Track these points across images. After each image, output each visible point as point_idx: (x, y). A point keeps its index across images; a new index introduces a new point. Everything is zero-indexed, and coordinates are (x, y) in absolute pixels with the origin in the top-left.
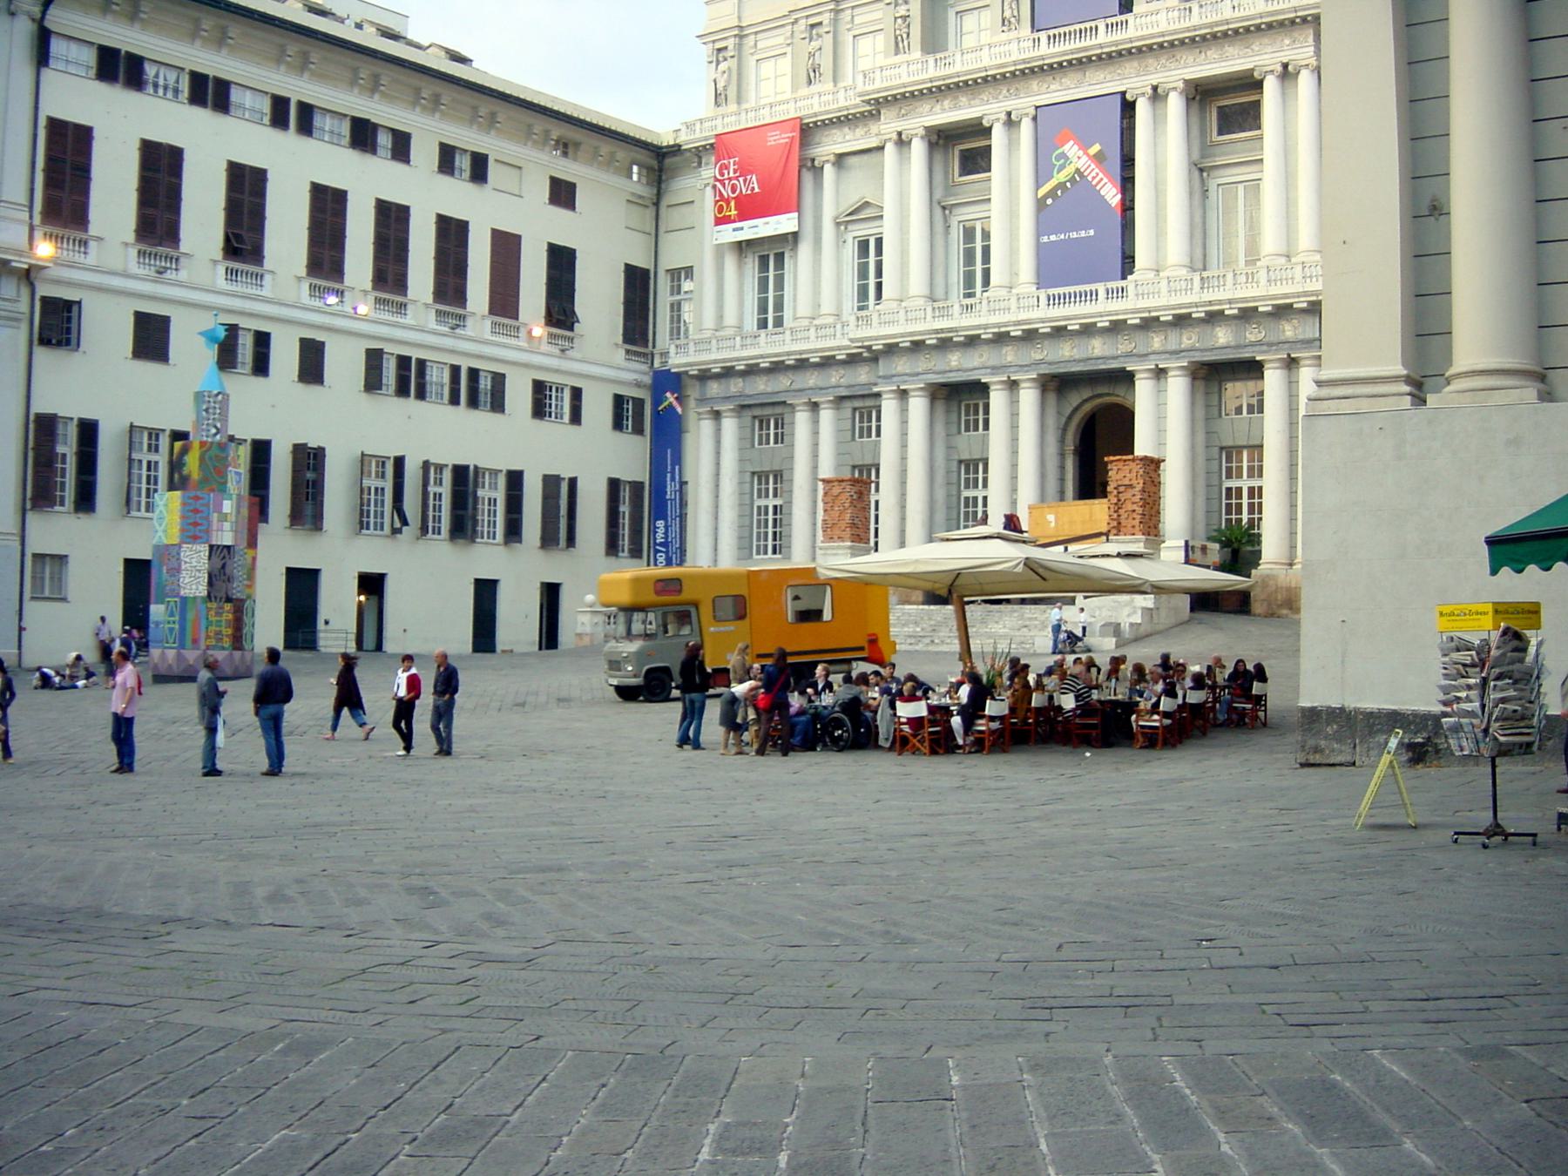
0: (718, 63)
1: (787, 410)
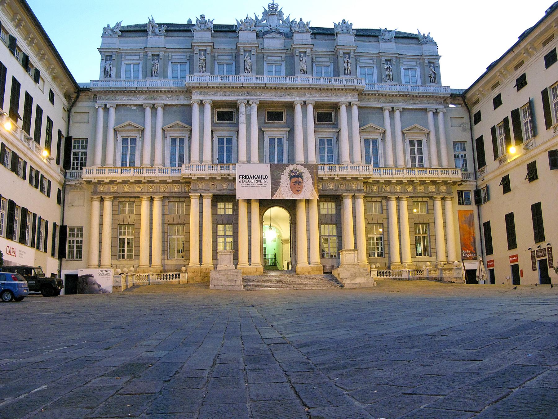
0: (106, 60)
1: (137, 200)
